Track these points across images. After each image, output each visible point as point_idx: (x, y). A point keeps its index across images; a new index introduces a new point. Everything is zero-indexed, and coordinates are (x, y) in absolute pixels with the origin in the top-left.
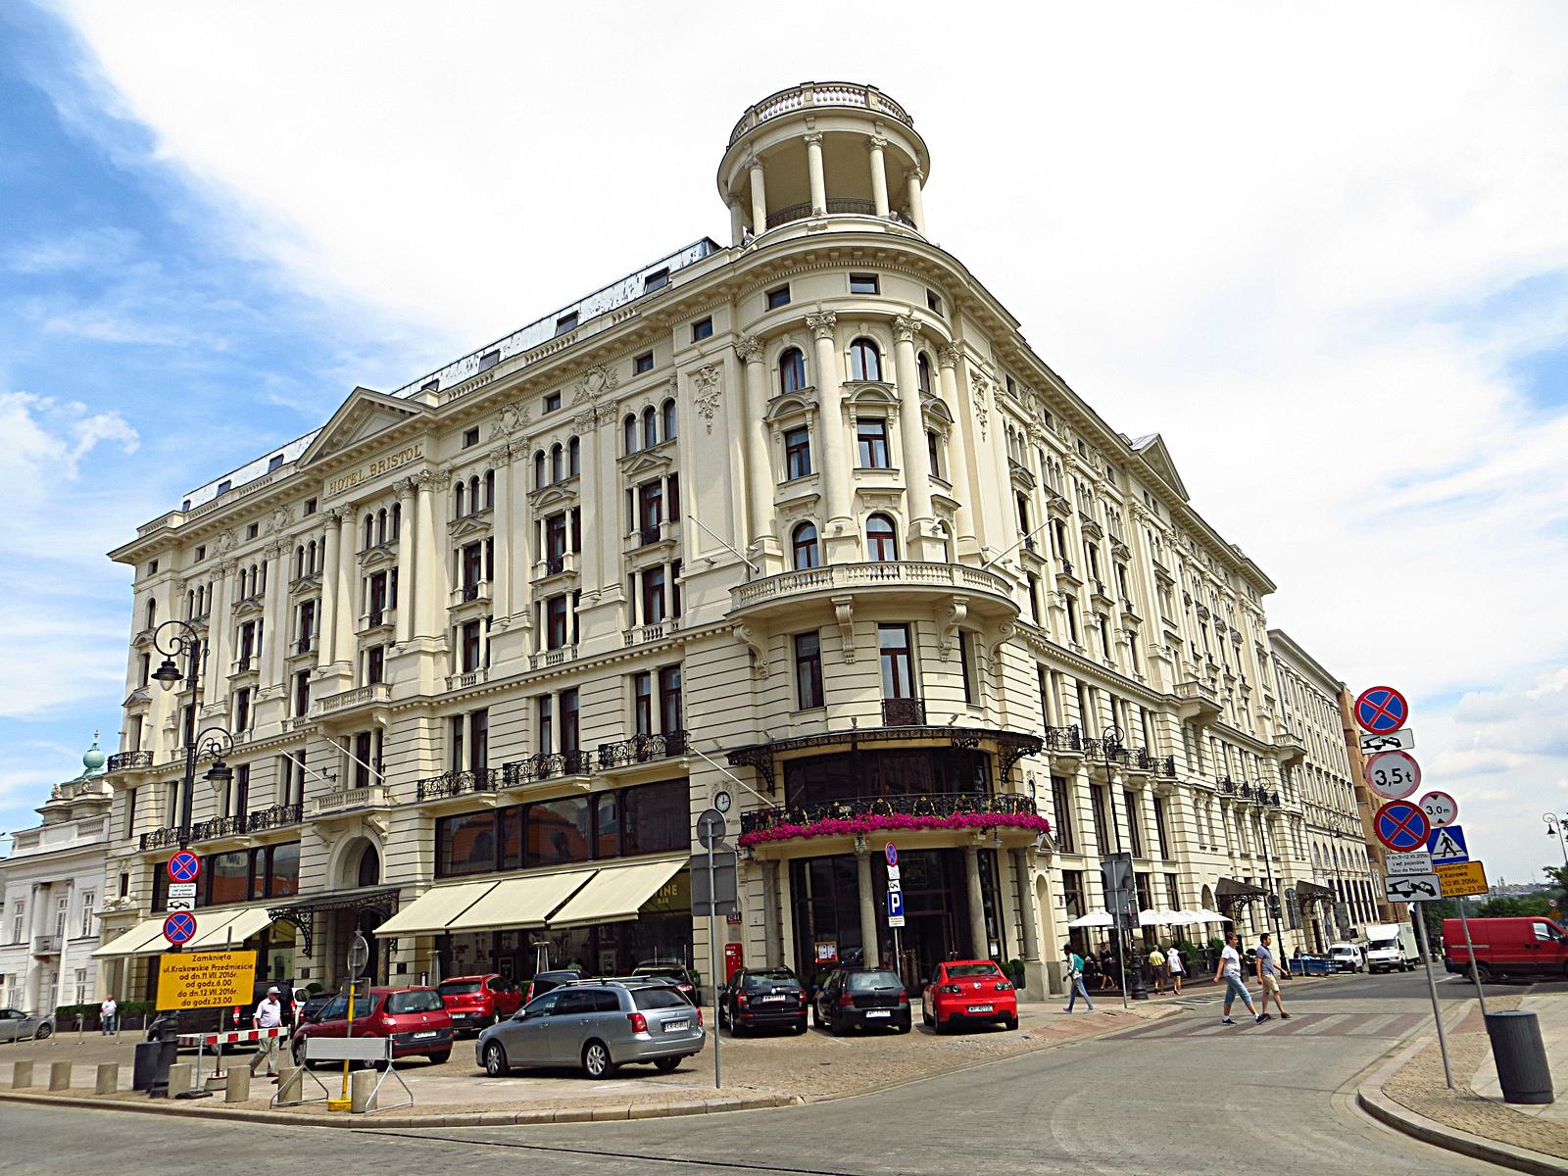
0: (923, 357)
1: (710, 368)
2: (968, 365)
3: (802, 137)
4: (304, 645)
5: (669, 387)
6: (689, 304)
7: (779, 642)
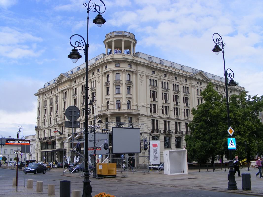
0: (129, 74)
1: (99, 77)
2: (138, 74)
3: (111, 41)
4: (57, 112)
5: (95, 78)
6: (97, 67)
7: (104, 119)
